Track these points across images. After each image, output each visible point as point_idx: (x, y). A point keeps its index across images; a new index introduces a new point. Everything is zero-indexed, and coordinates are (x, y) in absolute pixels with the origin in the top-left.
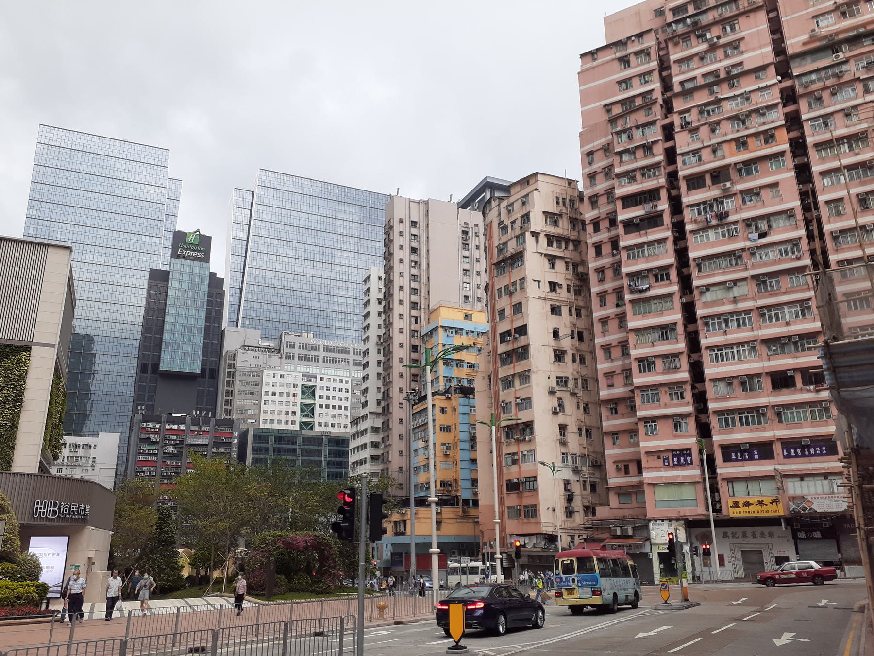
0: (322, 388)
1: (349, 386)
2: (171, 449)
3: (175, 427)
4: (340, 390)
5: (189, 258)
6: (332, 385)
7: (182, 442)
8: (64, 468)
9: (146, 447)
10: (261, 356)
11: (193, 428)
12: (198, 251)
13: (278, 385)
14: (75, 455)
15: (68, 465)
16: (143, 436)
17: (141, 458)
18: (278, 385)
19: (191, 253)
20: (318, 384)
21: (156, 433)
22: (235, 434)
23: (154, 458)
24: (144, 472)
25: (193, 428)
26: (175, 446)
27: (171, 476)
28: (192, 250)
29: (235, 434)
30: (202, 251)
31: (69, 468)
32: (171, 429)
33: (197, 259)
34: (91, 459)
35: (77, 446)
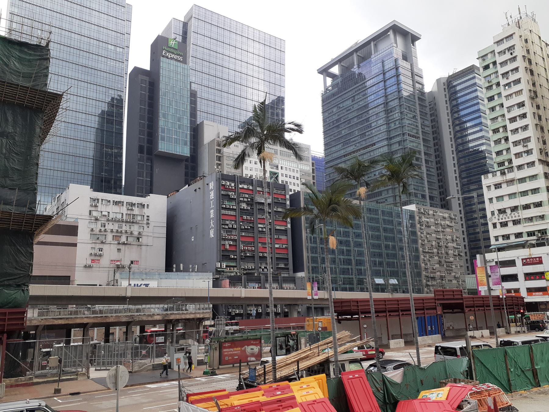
0: (282, 175)
1: (298, 175)
2: (244, 206)
3: (246, 187)
4: (294, 178)
5: (171, 58)
6: (289, 173)
7: (252, 199)
8: (124, 224)
9: (227, 204)
10: (239, 145)
11: (258, 189)
12: (178, 55)
13: (254, 169)
14: (132, 213)
15: (127, 222)
16: (223, 192)
17: (223, 212)
18: (254, 169)
19: (173, 56)
20: (280, 171)
21: (231, 190)
22: (288, 197)
23: (233, 213)
24: (227, 225)
25: (258, 189)
26: (248, 204)
27: (248, 229)
28: (173, 53)
29: (288, 197)
30: (181, 56)
31: (128, 225)
32: (243, 188)
33: (177, 60)
34: (146, 218)
35: (132, 205)
